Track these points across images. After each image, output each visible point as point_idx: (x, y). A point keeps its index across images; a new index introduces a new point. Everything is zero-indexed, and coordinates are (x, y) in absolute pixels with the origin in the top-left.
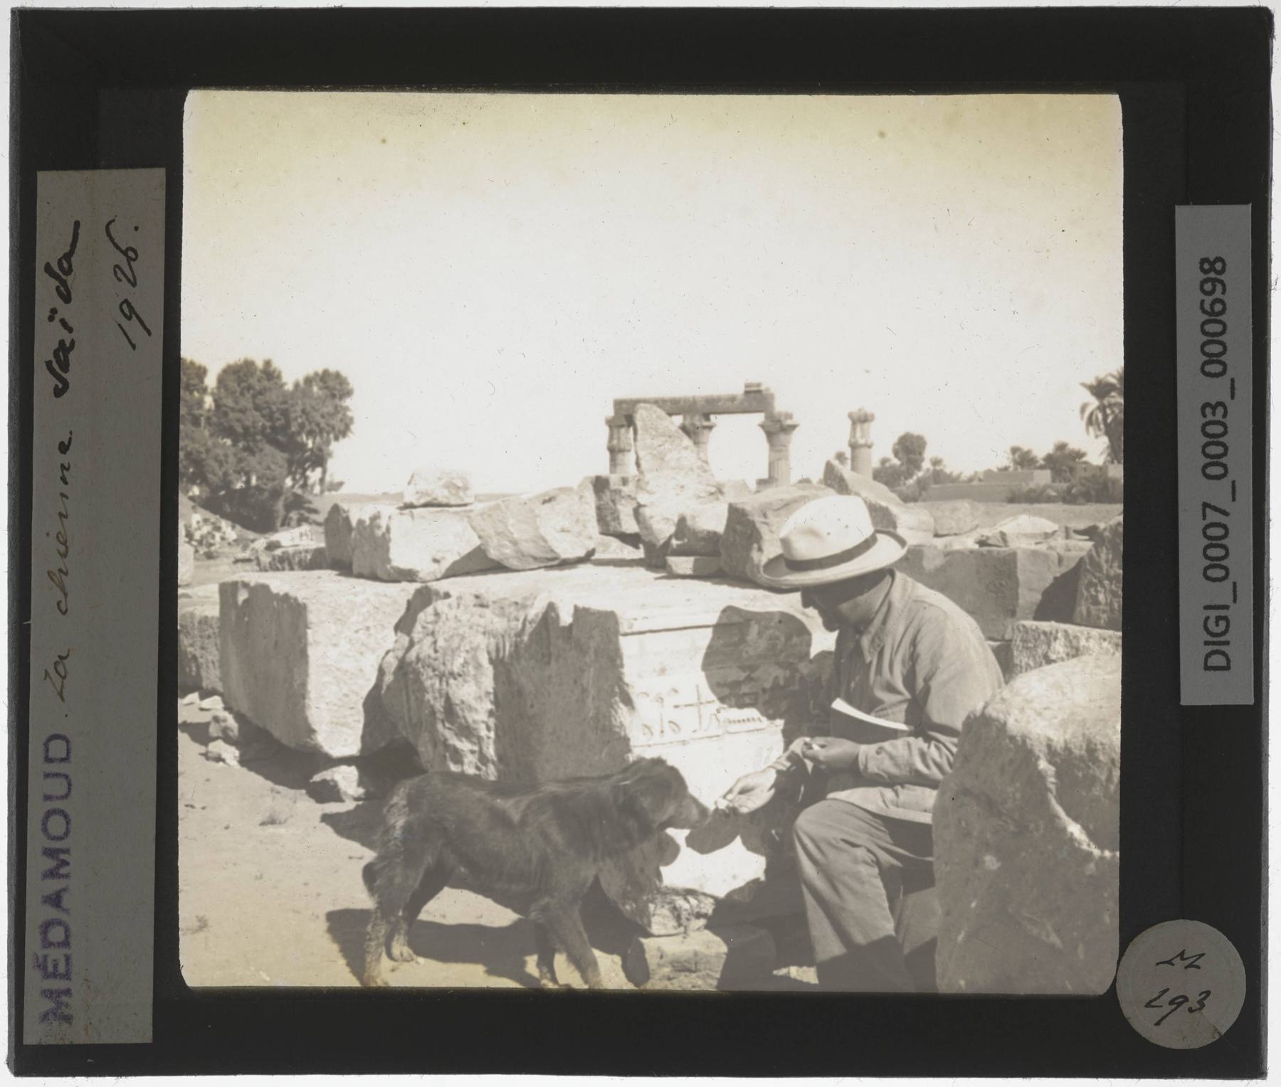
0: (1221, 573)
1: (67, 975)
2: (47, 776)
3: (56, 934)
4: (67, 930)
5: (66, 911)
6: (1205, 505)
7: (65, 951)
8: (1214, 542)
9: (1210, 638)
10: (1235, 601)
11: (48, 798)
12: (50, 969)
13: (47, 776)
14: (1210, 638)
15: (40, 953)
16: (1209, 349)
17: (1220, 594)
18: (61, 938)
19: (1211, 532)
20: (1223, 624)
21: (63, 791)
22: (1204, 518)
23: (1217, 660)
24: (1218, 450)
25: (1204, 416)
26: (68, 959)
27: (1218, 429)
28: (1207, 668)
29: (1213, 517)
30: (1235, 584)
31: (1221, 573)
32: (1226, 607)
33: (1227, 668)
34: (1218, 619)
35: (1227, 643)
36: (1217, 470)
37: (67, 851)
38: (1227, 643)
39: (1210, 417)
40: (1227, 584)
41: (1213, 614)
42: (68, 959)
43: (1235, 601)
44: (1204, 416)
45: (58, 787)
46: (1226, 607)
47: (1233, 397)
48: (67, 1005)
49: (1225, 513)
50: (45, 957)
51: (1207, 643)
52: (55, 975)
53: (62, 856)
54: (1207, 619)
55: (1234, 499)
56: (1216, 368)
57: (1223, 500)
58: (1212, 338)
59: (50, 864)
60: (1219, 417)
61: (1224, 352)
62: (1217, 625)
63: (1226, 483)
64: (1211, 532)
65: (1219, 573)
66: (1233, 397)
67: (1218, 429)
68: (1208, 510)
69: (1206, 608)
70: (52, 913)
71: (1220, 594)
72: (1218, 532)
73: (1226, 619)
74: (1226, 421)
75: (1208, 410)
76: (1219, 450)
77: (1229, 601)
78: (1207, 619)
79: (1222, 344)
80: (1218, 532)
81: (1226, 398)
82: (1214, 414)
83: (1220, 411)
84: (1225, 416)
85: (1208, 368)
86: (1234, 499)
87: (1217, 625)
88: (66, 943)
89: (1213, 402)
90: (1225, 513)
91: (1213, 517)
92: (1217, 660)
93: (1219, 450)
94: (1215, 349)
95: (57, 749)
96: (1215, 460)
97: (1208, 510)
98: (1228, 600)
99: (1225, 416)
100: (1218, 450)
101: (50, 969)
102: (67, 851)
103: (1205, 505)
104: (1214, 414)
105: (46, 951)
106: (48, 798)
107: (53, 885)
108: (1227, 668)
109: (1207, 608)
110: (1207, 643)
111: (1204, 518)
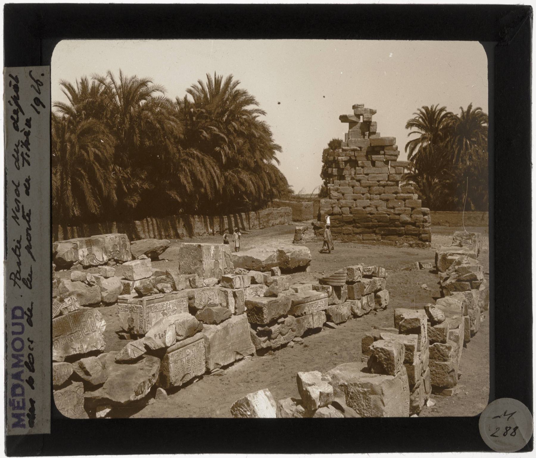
1: (23, 408)
2: (14, 324)
3: (19, 391)
4: (23, 389)
5: (22, 380)
7: (22, 397)
11: (13, 333)
12: (16, 405)
13: (14, 324)
15: (12, 399)
18: (21, 393)
21: (20, 330)
26: (23, 400)
37: (22, 356)
42: (23, 400)
45: (18, 329)
48: (23, 420)
50: (14, 400)
52: (19, 408)
53: (21, 358)
59: (16, 361)
70: (16, 382)
88: (23, 394)
95: (18, 313)
101: (16, 405)
102: (22, 356)
105: (14, 398)
106: (13, 333)
107: (16, 370)
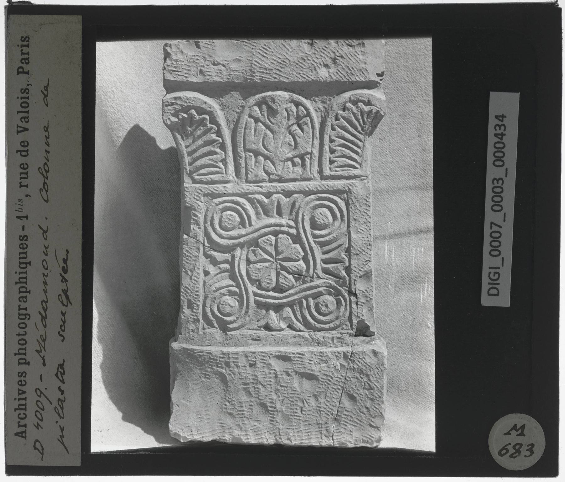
0: (497, 253)
6: (492, 223)
8: (496, 239)
9: (491, 282)
10: (503, 266)
14: (491, 282)
16: (497, 154)
17: (497, 262)
19: (493, 235)
20: (497, 276)
22: (491, 229)
23: (494, 291)
24: (499, 199)
25: (493, 184)
27: (499, 190)
28: (489, 294)
29: (495, 228)
30: (503, 258)
31: (497, 253)
32: (499, 268)
33: (498, 295)
34: (495, 273)
35: (498, 284)
36: (499, 208)
38: (498, 284)
39: (496, 184)
40: (499, 259)
41: (493, 271)
43: (503, 266)
44: (493, 184)
46: (499, 268)
47: (506, 176)
49: (500, 227)
51: (489, 284)
54: (490, 273)
55: (504, 221)
56: (500, 163)
57: (499, 221)
58: (499, 150)
60: (500, 184)
61: (503, 157)
62: (494, 276)
63: (502, 213)
64: (493, 235)
65: (496, 253)
66: (506, 176)
67: (499, 190)
68: (493, 225)
69: (490, 268)
71: (497, 262)
72: (497, 235)
73: (498, 273)
74: (503, 186)
75: (495, 182)
76: (499, 199)
77: (499, 265)
78: (490, 273)
79: (503, 153)
80: (497, 235)
81: (503, 176)
82: (498, 183)
83: (500, 182)
84: (502, 184)
85: (496, 163)
86: (504, 221)
87: (494, 276)
89: (498, 178)
90: (500, 227)
91: (495, 228)
92: (494, 291)
93: (499, 199)
94: (500, 155)
96: (497, 204)
97: (493, 225)
98: (499, 265)
99: (502, 184)
100: (499, 199)
103: (492, 223)
104: (498, 183)
108: (498, 295)
109: (490, 268)
110: (489, 284)
111: (491, 229)
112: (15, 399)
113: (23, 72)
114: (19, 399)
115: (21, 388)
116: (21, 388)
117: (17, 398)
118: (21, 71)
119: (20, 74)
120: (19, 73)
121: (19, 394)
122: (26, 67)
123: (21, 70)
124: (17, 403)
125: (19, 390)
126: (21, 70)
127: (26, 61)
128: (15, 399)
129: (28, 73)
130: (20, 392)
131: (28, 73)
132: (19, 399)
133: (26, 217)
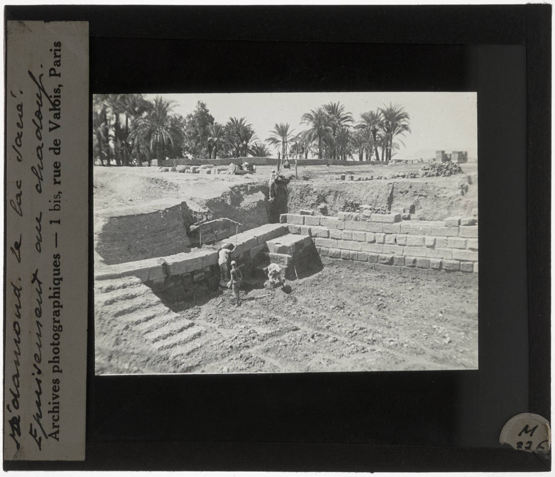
112: (50, 403)
113: (55, 75)
114: (54, 403)
115: (55, 393)
116: (55, 393)
117: (52, 401)
118: (53, 73)
119: (51, 77)
120: (51, 75)
121: (54, 399)
122: (58, 70)
123: (52, 72)
124: (52, 406)
125: (53, 394)
126: (52, 72)
127: (58, 63)
128: (50, 403)
129: (59, 75)
130: (54, 396)
131: (59, 75)
132: (54, 403)
133: (59, 222)
